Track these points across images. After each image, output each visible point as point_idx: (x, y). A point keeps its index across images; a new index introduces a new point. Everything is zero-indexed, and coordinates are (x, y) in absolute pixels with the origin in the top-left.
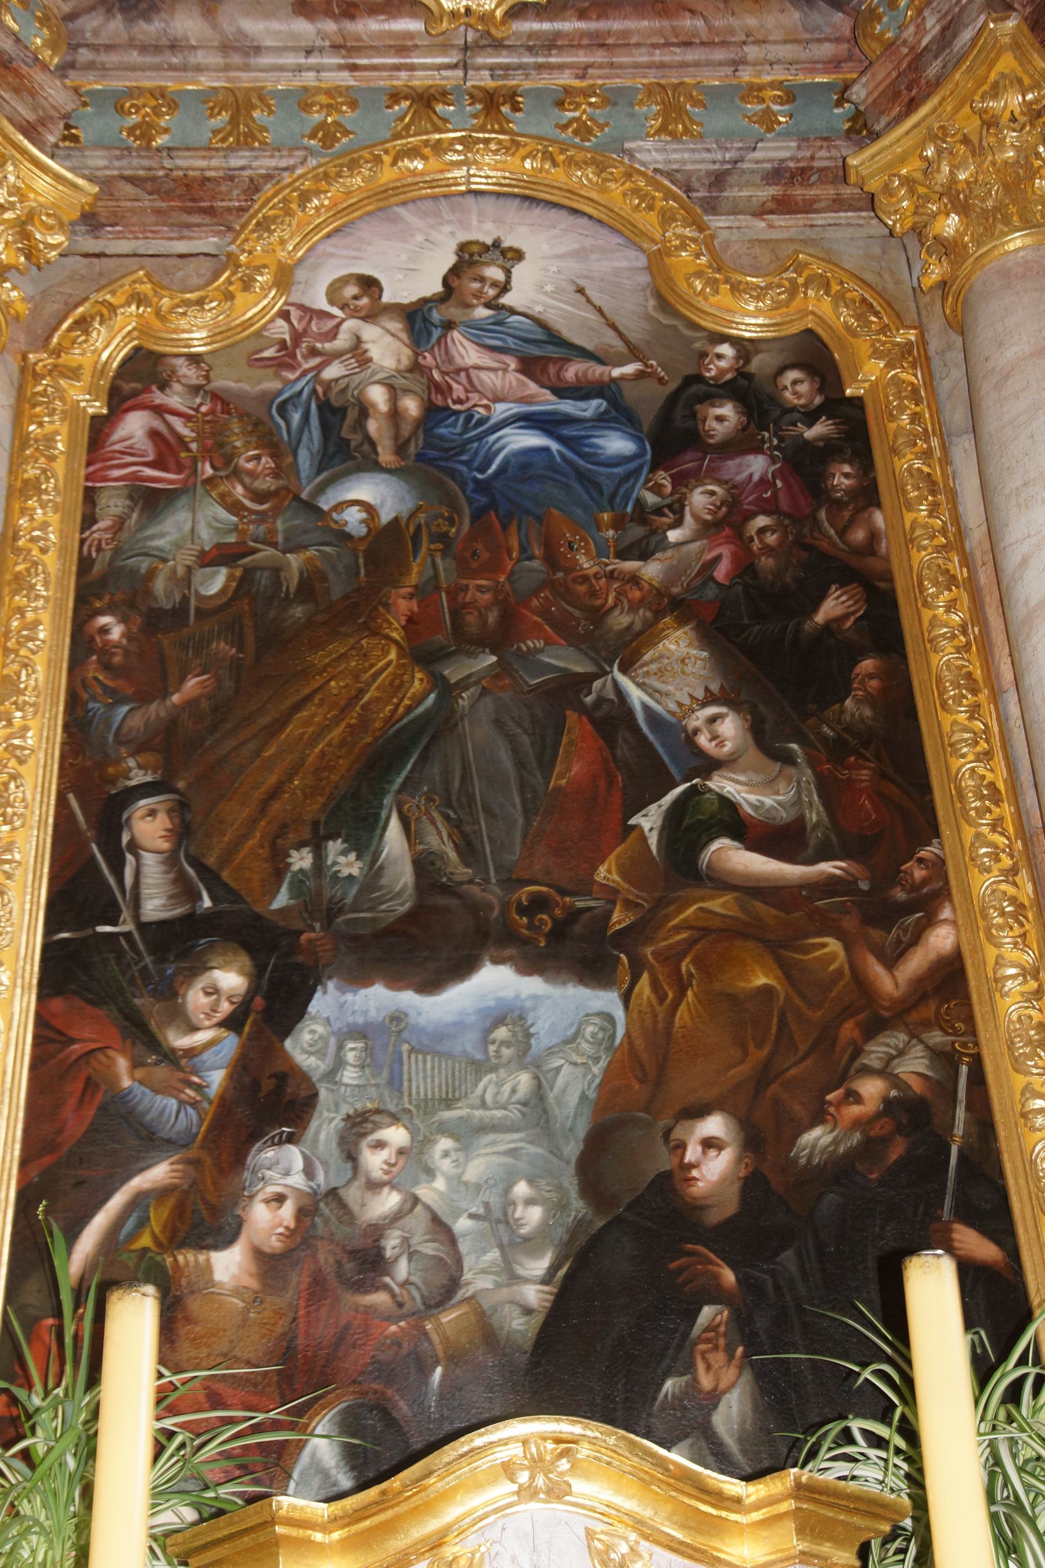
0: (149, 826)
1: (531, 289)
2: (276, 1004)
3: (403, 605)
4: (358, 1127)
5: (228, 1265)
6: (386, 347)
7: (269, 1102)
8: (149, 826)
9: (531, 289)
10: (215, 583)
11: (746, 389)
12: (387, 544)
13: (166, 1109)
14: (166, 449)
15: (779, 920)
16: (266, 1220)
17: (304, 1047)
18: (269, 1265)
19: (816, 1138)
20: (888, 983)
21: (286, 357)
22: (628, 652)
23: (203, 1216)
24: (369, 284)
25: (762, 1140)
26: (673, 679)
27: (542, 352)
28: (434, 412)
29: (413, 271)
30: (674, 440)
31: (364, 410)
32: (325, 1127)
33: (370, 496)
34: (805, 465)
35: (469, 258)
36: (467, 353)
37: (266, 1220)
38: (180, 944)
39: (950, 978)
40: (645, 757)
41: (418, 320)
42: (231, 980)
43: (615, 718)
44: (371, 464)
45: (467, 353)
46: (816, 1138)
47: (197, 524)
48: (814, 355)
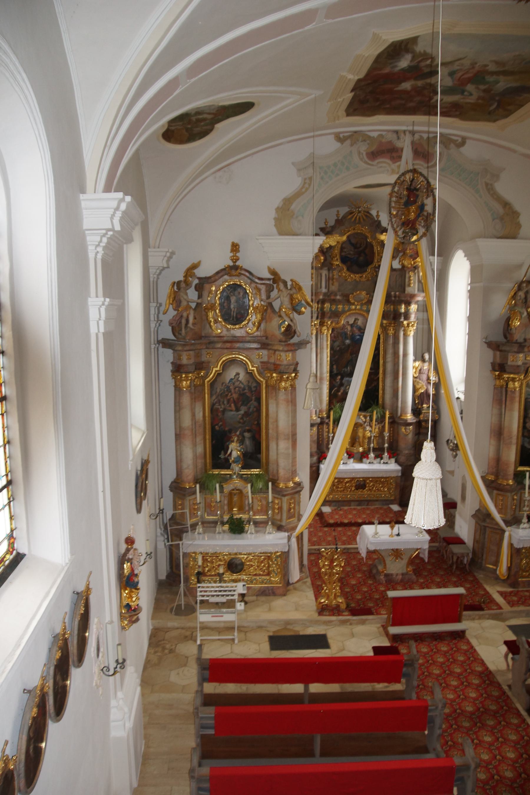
0: (335, 367)
2: (342, 379)
3: (350, 351)
4: (346, 386)
5: (340, 393)
6: (349, 328)
7: (342, 385)
8: (335, 367)
10: (338, 348)
12: (349, 346)
13: (336, 385)
14: (335, 337)
16: (342, 391)
17: (344, 381)
18: (342, 394)
19: (370, 388)
20: (376, 378)
21: (342, 329)
23: (338, 391)
24: (348, 322)
28: (352, 334)
29: (351, 321)
31: (347, 334)
32: (345, 386)
33: (348, 342)
36: (355, 329)
37: (342, 391)
38: (337, 375)
39: (379, 378)
41: (352, 326)
42: (339, 377)
44: (348, 339)
45: (355, 329)
46: (370, 388)
47: (337, 344)
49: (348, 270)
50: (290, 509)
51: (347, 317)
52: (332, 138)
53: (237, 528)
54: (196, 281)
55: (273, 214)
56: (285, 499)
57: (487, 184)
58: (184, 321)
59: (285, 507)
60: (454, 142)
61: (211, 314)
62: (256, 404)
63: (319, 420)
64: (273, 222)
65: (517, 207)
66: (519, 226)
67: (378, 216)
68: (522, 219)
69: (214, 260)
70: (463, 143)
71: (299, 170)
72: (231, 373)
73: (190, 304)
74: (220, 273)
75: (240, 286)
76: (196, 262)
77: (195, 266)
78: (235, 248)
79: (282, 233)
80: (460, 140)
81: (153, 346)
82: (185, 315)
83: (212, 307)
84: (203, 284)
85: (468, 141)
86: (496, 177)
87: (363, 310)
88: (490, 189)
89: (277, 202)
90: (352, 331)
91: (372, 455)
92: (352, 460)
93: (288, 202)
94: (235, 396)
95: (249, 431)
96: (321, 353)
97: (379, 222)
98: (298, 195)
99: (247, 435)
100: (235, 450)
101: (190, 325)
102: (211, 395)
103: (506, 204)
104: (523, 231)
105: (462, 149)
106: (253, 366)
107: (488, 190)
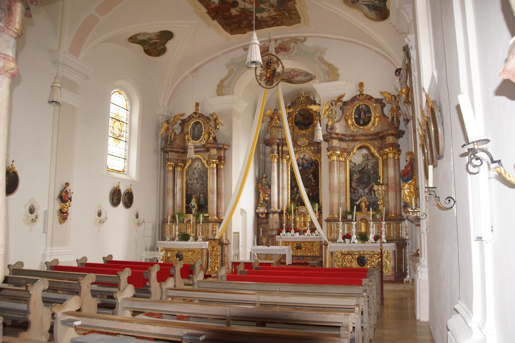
1: (306, 157)
6: (301, 160)
9: (306, 157)
11: (314, 162)
15: (313, 186)
22: (309, 175)
25: (312, 194)
26: (311, 176)
27: (307, 160)
29: (302, 157)
30: (311, 165)
34: (316, 166)
35: (304, 155)
40: (310, 179)
43: (309, 178)
48: (317, 161)
49: (299, 128)
50: (213, 231)
51: (299, 154)
52: (242, 49)
53: (185, 237)
54: (181, 121)
55: (216, 88)
56: (210, 225)
57: (319, 57)
58: (169, 138)
59: (210, 230)
60: (300, 40)
61: (187, 137)
62: (206, 180)
63: (279, 211)
64: (216, 92)
65: (337, 66)
66: (338, 75)
67: (314, 98)
68: (340, 72)
69: (189, 111)
70: (305, 40)
71: (227, 67)
72: (195, 165)
73: (175, 130)
74: (190, 117)
75: (199, 122)
76: (182, 113)
77: (182, 115)
78: (197, 105)
79: (218, 95)
80: (303, 39)
81: (159, 152)
82: (170, 135)
83: (188, 133)
84: (184, 123)
85: (307, 39)
86: (323, 52)
87: (308, 150)
88: (321, 59)
89: (218, 82)
90: (302, 162)
91: (309, 232)
92: (298, 234)
93: (222, 81)
94: (196, 176)
95: (202, 193)
96: (283, 174)
97: (315, 101)
98: (227, 77)
99: (201, 195)
100: (193, 203)
101: (172, 140)
102: (186, 176)
103: (329, 65)
104: (340, 78)
105: (304, 43)
106: (204, 160)
107: (320, 61)
